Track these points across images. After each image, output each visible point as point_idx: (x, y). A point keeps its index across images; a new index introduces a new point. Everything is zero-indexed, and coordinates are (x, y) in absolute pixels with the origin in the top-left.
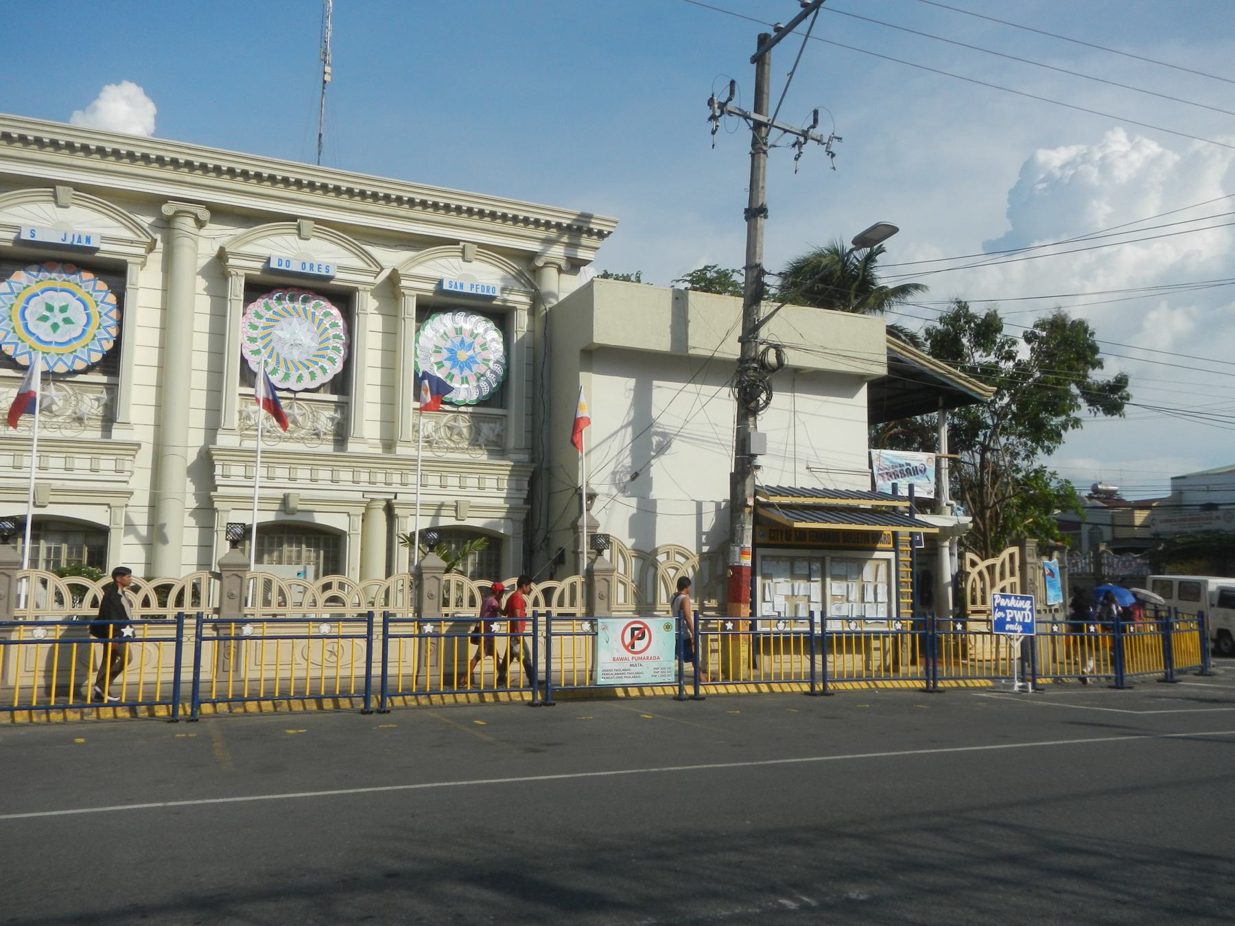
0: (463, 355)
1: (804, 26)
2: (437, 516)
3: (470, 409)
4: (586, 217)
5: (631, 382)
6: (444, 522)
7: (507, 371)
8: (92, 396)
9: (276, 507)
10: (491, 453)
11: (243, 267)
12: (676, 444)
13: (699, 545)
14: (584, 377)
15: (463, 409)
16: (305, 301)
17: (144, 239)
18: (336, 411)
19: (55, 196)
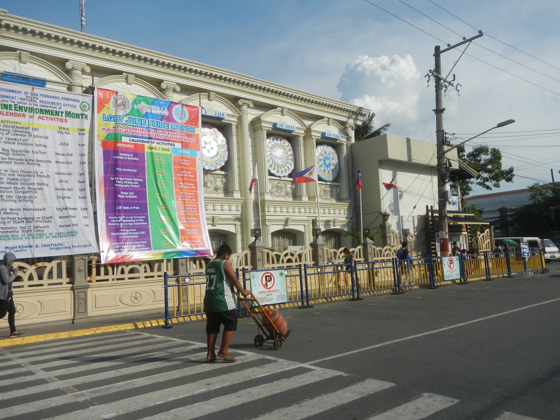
0: (327, 162)
1: (464, 46)
3: (330, 183)
4: (361, 109)
5: (391, 172)
7: (339, 168)
8: (220, 180)
9: (283, 223)
11: (267, 126)
12: (405, 195)
13: (415, 232)
14: (380, 170)
15: (328, 183)
16: (281, 140)
17: (236, 115)
18: (292, 185)
19: (209, 96)
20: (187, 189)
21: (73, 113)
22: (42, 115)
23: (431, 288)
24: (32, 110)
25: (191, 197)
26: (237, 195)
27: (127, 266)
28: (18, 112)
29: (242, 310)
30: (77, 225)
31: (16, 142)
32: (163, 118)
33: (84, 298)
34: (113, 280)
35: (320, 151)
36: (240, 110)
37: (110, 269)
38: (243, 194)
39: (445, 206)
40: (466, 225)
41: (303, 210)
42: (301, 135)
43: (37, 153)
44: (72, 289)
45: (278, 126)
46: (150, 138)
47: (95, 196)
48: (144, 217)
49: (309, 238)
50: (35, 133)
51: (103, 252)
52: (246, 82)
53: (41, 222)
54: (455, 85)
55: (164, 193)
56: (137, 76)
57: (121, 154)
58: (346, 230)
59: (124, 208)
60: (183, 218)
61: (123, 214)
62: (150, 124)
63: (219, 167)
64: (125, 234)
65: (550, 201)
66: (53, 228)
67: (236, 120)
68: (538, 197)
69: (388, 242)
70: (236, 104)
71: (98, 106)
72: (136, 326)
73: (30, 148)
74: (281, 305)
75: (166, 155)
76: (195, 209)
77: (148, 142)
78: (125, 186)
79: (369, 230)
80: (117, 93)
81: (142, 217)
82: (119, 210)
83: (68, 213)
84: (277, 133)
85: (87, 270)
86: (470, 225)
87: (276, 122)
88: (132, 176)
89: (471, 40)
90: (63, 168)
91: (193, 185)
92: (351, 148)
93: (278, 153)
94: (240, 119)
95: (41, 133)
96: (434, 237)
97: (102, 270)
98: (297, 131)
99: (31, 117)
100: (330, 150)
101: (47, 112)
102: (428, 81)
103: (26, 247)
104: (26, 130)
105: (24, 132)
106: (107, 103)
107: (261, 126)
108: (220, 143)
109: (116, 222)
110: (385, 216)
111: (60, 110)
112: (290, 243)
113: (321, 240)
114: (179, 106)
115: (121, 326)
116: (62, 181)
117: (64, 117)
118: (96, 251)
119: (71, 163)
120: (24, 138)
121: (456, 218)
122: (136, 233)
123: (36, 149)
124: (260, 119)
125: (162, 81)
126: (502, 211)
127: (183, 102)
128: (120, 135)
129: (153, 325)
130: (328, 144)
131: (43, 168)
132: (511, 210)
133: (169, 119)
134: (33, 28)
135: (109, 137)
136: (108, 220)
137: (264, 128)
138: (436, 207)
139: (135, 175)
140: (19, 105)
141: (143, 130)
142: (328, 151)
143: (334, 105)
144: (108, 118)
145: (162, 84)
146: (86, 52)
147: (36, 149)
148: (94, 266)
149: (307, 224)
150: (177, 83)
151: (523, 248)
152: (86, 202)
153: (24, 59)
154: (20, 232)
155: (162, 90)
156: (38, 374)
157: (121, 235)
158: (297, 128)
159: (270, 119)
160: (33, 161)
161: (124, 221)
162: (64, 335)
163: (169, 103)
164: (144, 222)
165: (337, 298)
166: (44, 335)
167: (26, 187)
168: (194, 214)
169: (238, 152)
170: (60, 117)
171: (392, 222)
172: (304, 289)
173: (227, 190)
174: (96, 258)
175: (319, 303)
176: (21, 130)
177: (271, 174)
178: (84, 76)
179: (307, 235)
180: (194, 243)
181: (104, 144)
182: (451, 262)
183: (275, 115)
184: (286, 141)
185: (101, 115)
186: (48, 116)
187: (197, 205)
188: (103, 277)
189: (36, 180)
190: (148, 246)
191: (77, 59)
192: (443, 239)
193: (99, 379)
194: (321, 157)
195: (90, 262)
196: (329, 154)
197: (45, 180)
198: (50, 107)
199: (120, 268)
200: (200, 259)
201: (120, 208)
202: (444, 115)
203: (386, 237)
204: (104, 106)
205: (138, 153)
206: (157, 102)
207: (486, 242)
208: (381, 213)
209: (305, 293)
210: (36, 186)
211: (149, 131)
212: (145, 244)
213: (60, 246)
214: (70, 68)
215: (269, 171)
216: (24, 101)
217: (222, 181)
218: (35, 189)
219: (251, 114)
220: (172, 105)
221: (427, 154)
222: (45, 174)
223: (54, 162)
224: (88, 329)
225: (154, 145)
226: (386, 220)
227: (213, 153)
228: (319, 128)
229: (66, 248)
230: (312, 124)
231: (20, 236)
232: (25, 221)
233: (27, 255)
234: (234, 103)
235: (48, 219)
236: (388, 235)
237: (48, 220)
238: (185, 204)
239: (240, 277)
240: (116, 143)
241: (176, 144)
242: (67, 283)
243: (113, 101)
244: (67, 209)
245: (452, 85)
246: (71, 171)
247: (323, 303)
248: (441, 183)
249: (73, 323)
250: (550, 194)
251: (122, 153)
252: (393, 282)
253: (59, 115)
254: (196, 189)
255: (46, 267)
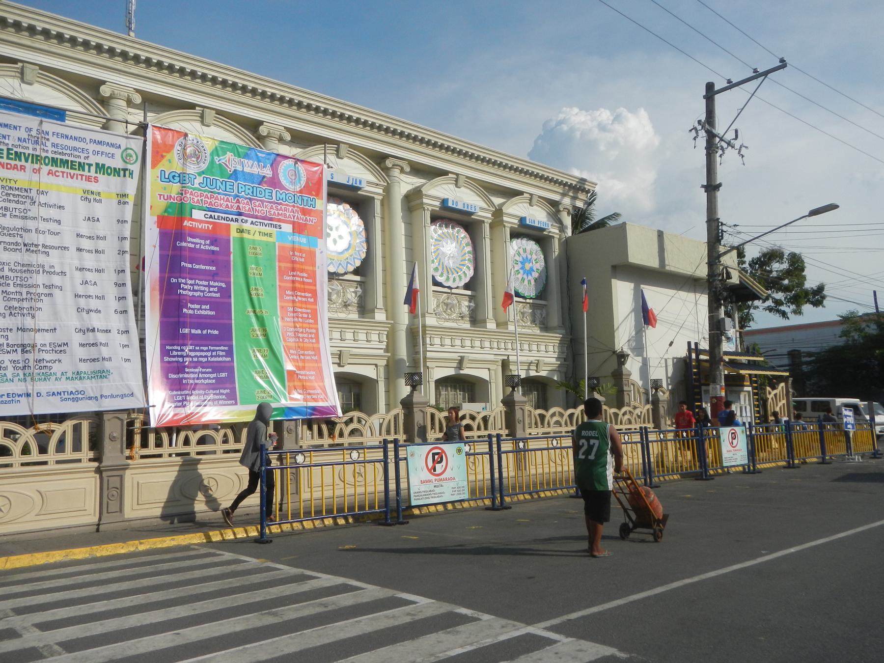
0: (528, 266)
2: (529, 369)
3: (531, 301)
4: (583, 181)
5: (632, 285)
6: (533, 373)
7: (547, 277)
8: (352, 290)
9: (455, 365)
10: (542, 329)
11: (431, 204)
13: (668, 385)
14: (613, 280)
15: (528, 301)
16: (453, 228)
17: (382, 183)
18: (470, 302)
19: (338, 150)
20: (301, 302)
21: (109, 167)
22: (54, 169)
23: (702, 479)
24: (37, 159)
25: (306, 316)
26: (380, 316)
27: (195, 431)
28: (13, 162)
29: (392, 511)
30: (110, 359)
31: (8, 213)
32: (262, 180)
33: (119, 487)
34: (170, 455)
35: (516, 248)
36: (388, 176)
37: (165, 436)
38: (391, 312)
39: (719, 342)
40: (750, 375)
41: (487, 344)
42: (486, 220)
43: (44, 233)
44: (98, 471)
45: (450, 204)
46: (240, 214)
47: (143, 311)
48: (226, 348)
49: (497, 392)
50: (43, 199)
51: (154, 406)
52: (399, 129)
53: (47, 352)
54: (737, 146)
55: (260, 307)
56: (219, 112)
57: (189, 239)
58: (555, 378)
59: (193, 331)
60: (292, 351)
61: (190, 342)
62: (240, 190)
63: (351, 268)
64: (190, 376)
65: (873, 342)
66: (66, 365)
67: (381, 191)
68: (852, 334)
69: (626, 400)
70: (382, 166)
71: (153, 157)
72: (208, 537)
73: (31, 224)
74: (456, 504)
75: (267, 244)
76: (313, 336)
77: (237, 220)
78: (196, 294)
79: (597, 379)
80: (186, 135)
81: (222, 348)
82: (184, 334)
83: (95, 337)
84: (448, 216)
85: (125, 438)
86: (756, 376)
87: (446, 197)
88: (208, 278)
89: (766, 74)
90: (89, 261)
91: (310, 295)
92: (566, 244)
93: (448, 248)
94: (388, 190)
95: (52, 199)
96: (700, 394)
97: (152, 437)
98: (480, 214)
99: (35, 171)
100: (531, 246)
101: (64, 163)
102: (695, 139)
103: (20, 395)
104: (25, 194)
105: (22, 197)
106: (168, 151)
107: (422, 203)
108: (354, 228)
109: (178, 356)
110: (622, 358)
111: (86, 161)
112: (464, 398)
113: (518, 395)
114: (291, 162)
115: (182, 537)
116: (86, 282)
117: (93, 173)
118: (142, 405)
119: (103, 252)
120: (22, 207)
121: (733, 364)
122: (214, 375)
123: (43, 226)
124: (420, 191)
125: (261, 123)
126: (794, 355)
127: (297, 157)
128: (188, 208)
129: (239, 536)
130: (530, 237)
131: (54, 259)
132: (810, 354)
133: (274, 182)
134: (47, 26)
135: (170, 210)
136: (164, 353)
137: (426, 207)
138: (705, 345)
139: (213, 276)
140: (15, 149)
141: (228, 200)
142: (528, 248)
143: (541, 173)
144: (169, 178)
145: (261, 128)
146: (135, 70)
147: (43, 226)
148: (138, 430)
149: (492, 367)
150: (285, 128)
151: (846, 416)
152: (127, 320)
153: (28, 76)
154: (10, 368)
155: (261, 138)
156: (26, 635)
157: (185, 379)
158: (481, 208)
159: (438, 191)
160: (37, 246)
161: (192, 354)
162: (80, 553)
163: (273, 156)
164: (226, 356)
165: (548, 494)
166: (45, 554)
167: (24, 291)
168: (311, 345)
169: (383, 244)
170: (86, 173)
171: (632, 366)
172: (496, 475)
173: (364, 308)
174: (141, 417)
175: (519, 502)
176: (17, 193)
177: (436, 283)
178: (130, 110)
179: (493, 385)
180: (309, 394)
181: (162, 221)
182: (734, 436)
183: (445, 186)
184: (462, 230)
185: (157, 171)
186: (65, 170)
187: (317, 329)
188: (152, 450)
189: (40, 279)
190: (232, 397)
191: (121, 81)
192: (716, 398)
193: (142, 650)
194: (517, 258)
195: (131, 424)
196: (531, 254)
197: (56, 280)
198: (69, 155)
199: (182, 435)
200: (319, 422)
201: (186, 331)
202: (720, 195)
203: (623, 391)
204: (163, 157)
205: (219, 238)
206: (253, 154)
207: (780, 404)
208: (614, 352)
209: (497, 482)
210: (41, 290)
211: (238, 201)
212: (226, 395)
213: (80, 396)
214: (107, 95)
215: (433, 277)
216: (24, 144)
217: (355, 292)
218: (39, 295)
219: (405, 184)
220: (279, 159)
221: (691, 259)
222: (57, 270)
223: (73, 249)
224: (124, 542)
225: (246, 226)
226: (623, 363)
227: (342, 245)
228: (516, 210)
229: (90, 398)
230: (504, 204)
231: (9, 376)
232: (19, 350)
233: (21, 409)
234: (378, 164)
235: (61, 347)
236: (625, 388)
237: (60, 349)
238: (295, 327)
239: (389, 453)
240: (181, 220)
241: (283, 225)
242: (90, 460)
243: (179, 148)
244: (93, 330)
245: (733, 147)
246: (102, 266)
247: (525, 501)
248: (713, 307)
249: (98, 530)
250: (873, 329)
251: (193, 237)
252: (641, 467)
253: (84, 170)
254: (315, 303)
255: (53, 431)
